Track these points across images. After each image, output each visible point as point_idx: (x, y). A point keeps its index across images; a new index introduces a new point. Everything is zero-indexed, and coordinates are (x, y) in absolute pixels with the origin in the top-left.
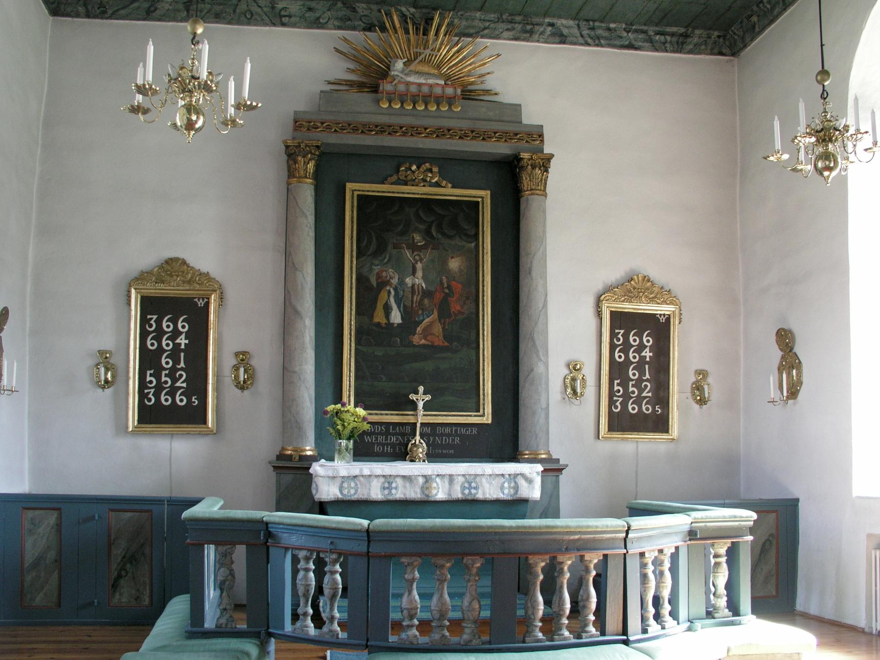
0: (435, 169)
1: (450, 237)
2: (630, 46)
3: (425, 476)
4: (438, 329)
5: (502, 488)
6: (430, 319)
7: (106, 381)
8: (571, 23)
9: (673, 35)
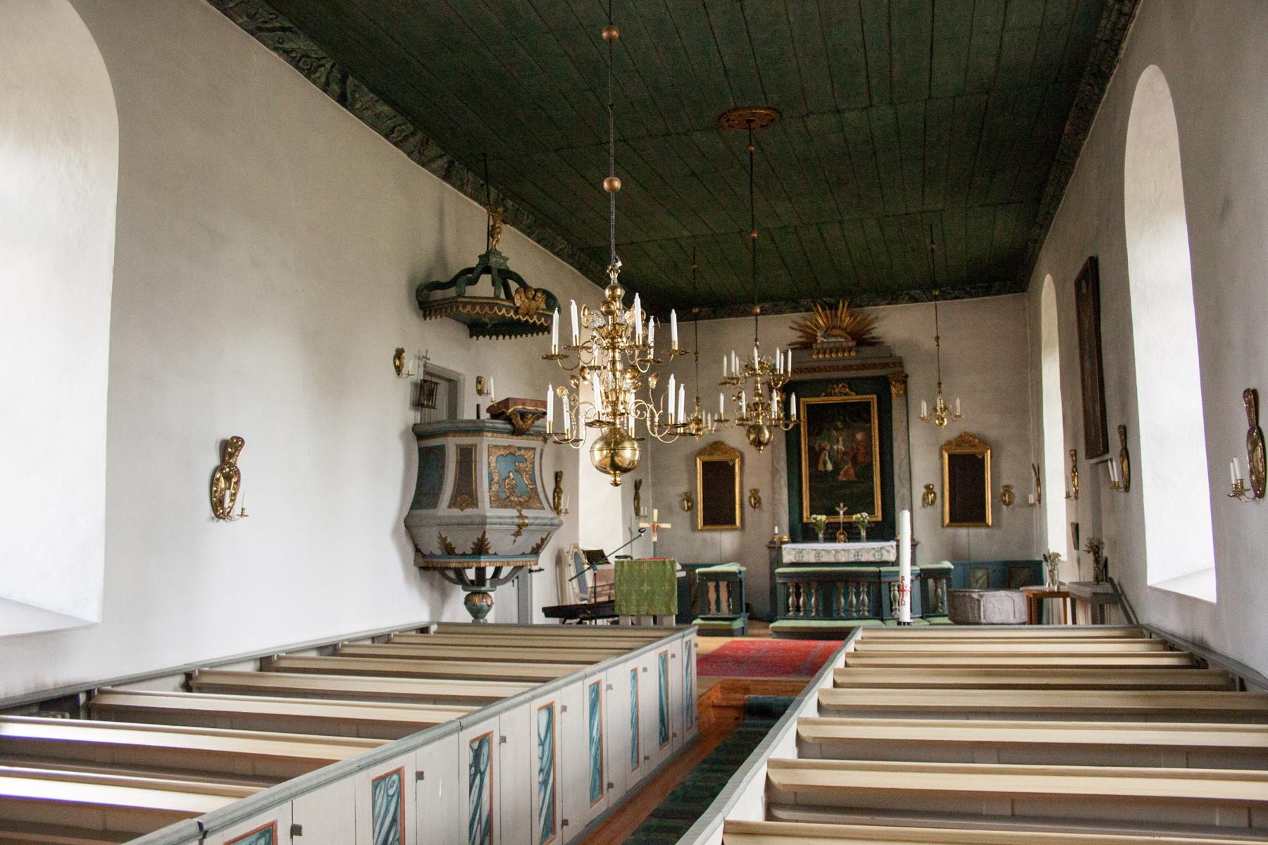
0: (847, 386)
1: (855, 421)
2: (956, 298)
3: (835, 550)
4: (852, 471)
5: (874, 556)
6: (847, 467)
7: (688, 508)
8: (918, 291)
9: (981, 287)
